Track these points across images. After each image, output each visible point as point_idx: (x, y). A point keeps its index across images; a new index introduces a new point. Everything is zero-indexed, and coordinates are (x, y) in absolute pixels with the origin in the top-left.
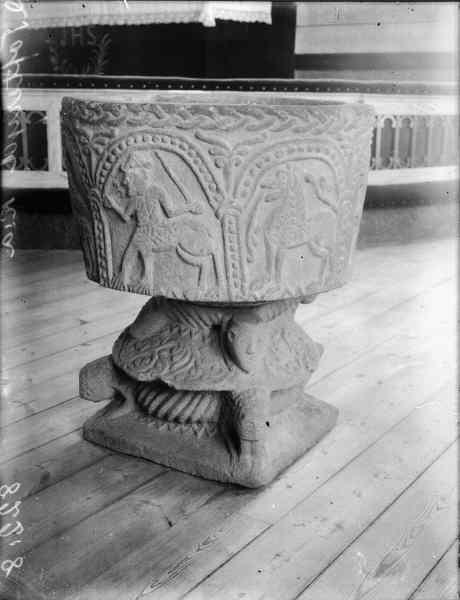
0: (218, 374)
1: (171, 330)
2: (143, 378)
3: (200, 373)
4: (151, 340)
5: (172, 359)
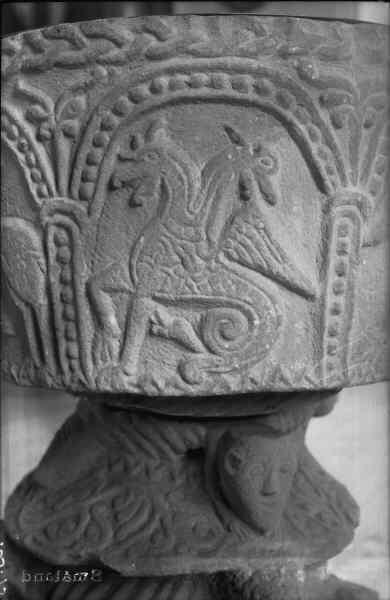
0: (207, 539)
1: (110, 466)
5: (116, 517)
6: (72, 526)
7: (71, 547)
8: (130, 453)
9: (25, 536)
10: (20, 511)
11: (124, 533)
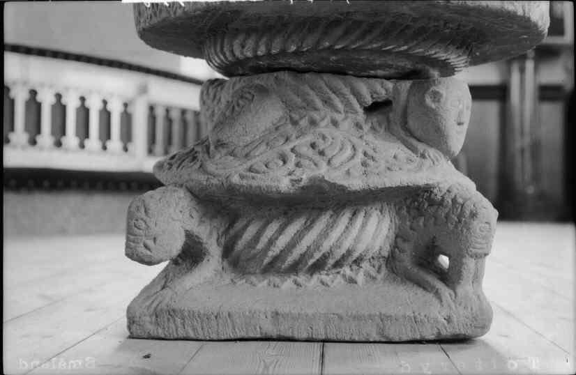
2: (285, 185)
5: (322, 153)
7: (290, 174)
8: (316, 109)
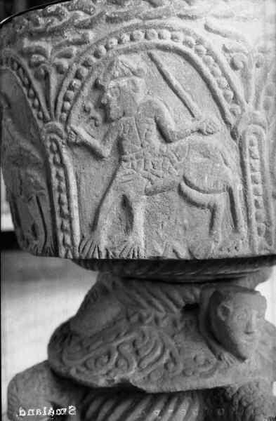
0: (205, 365)
1: (128, 318)
2: (102, 382)
3: (181, 367)
4: (101, 335)
5: (137, 353)
6: (105, 360)
7: (107, 374)
8: (143, 308)
9: (70, 368)
10: (62, 352)
11: (145, 363)
